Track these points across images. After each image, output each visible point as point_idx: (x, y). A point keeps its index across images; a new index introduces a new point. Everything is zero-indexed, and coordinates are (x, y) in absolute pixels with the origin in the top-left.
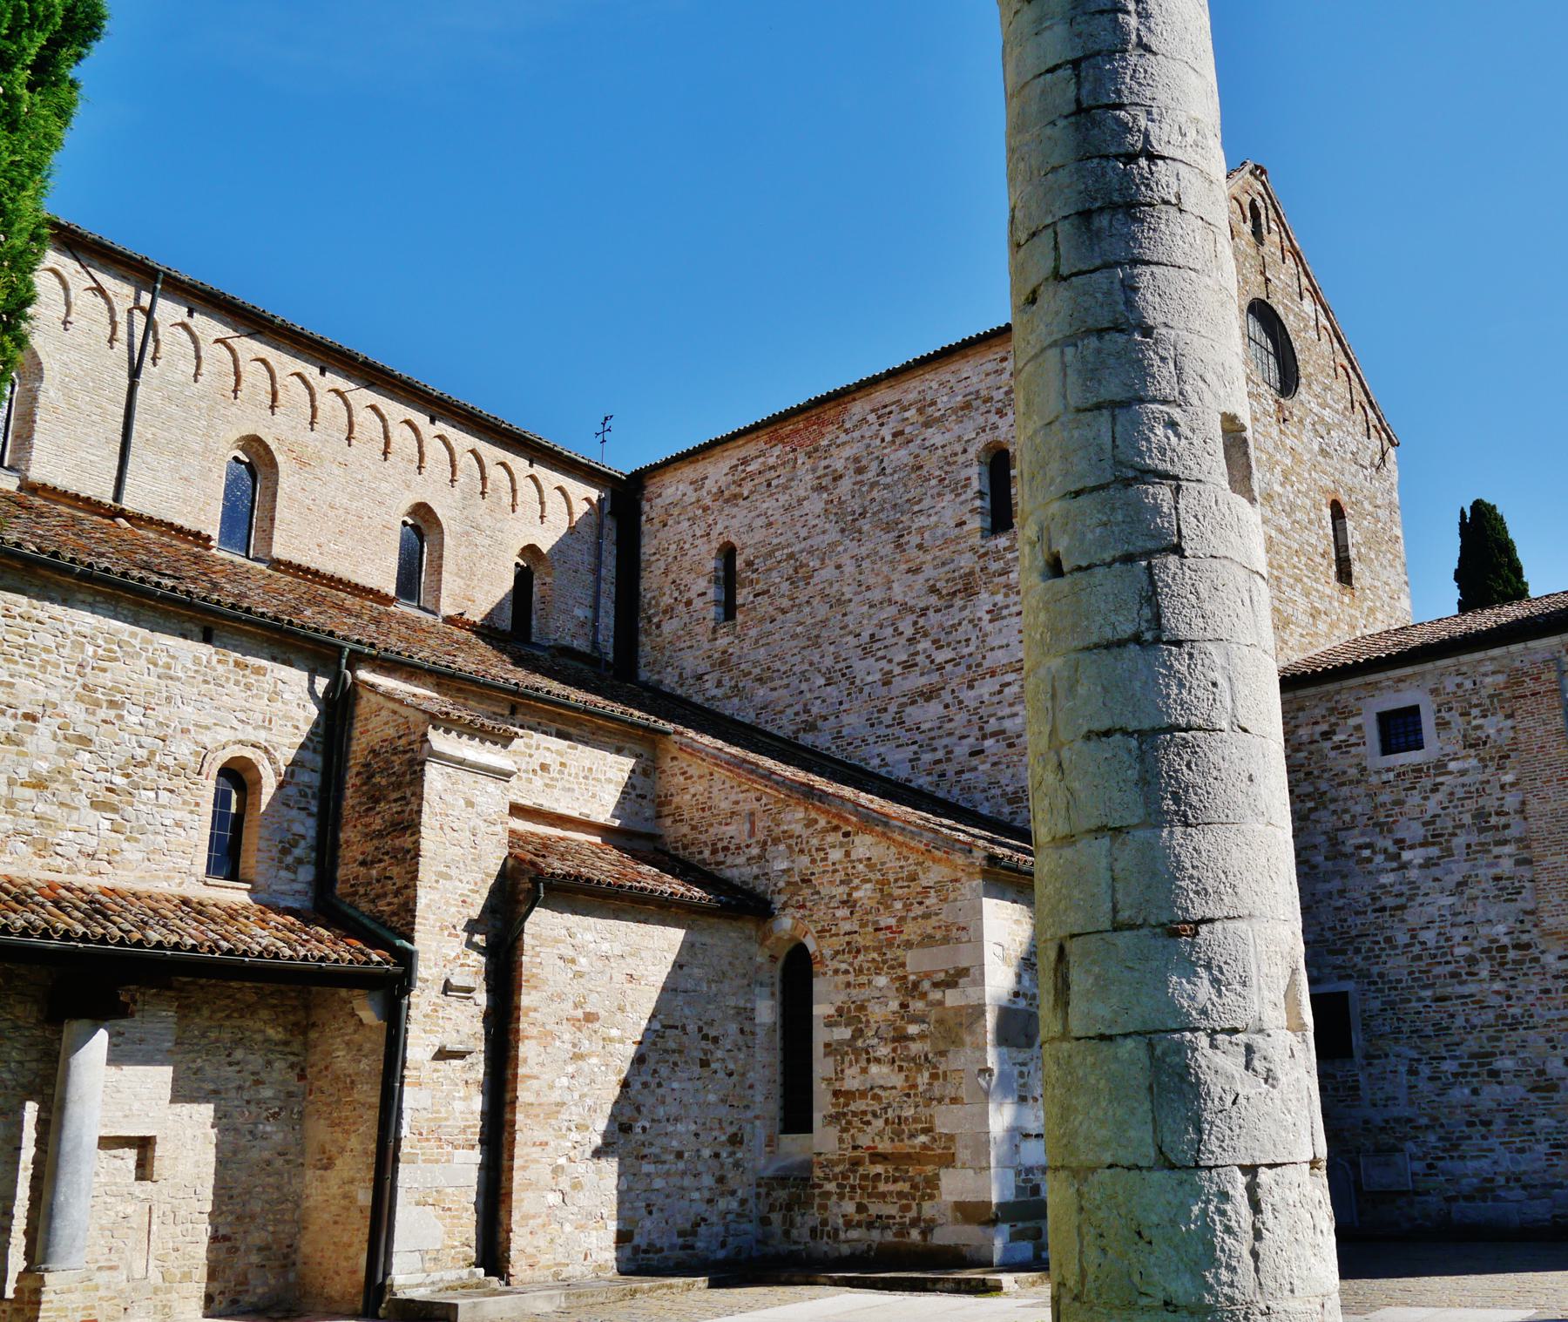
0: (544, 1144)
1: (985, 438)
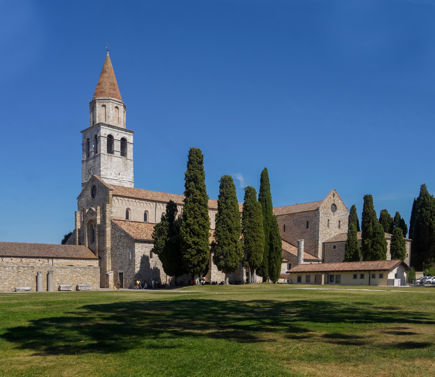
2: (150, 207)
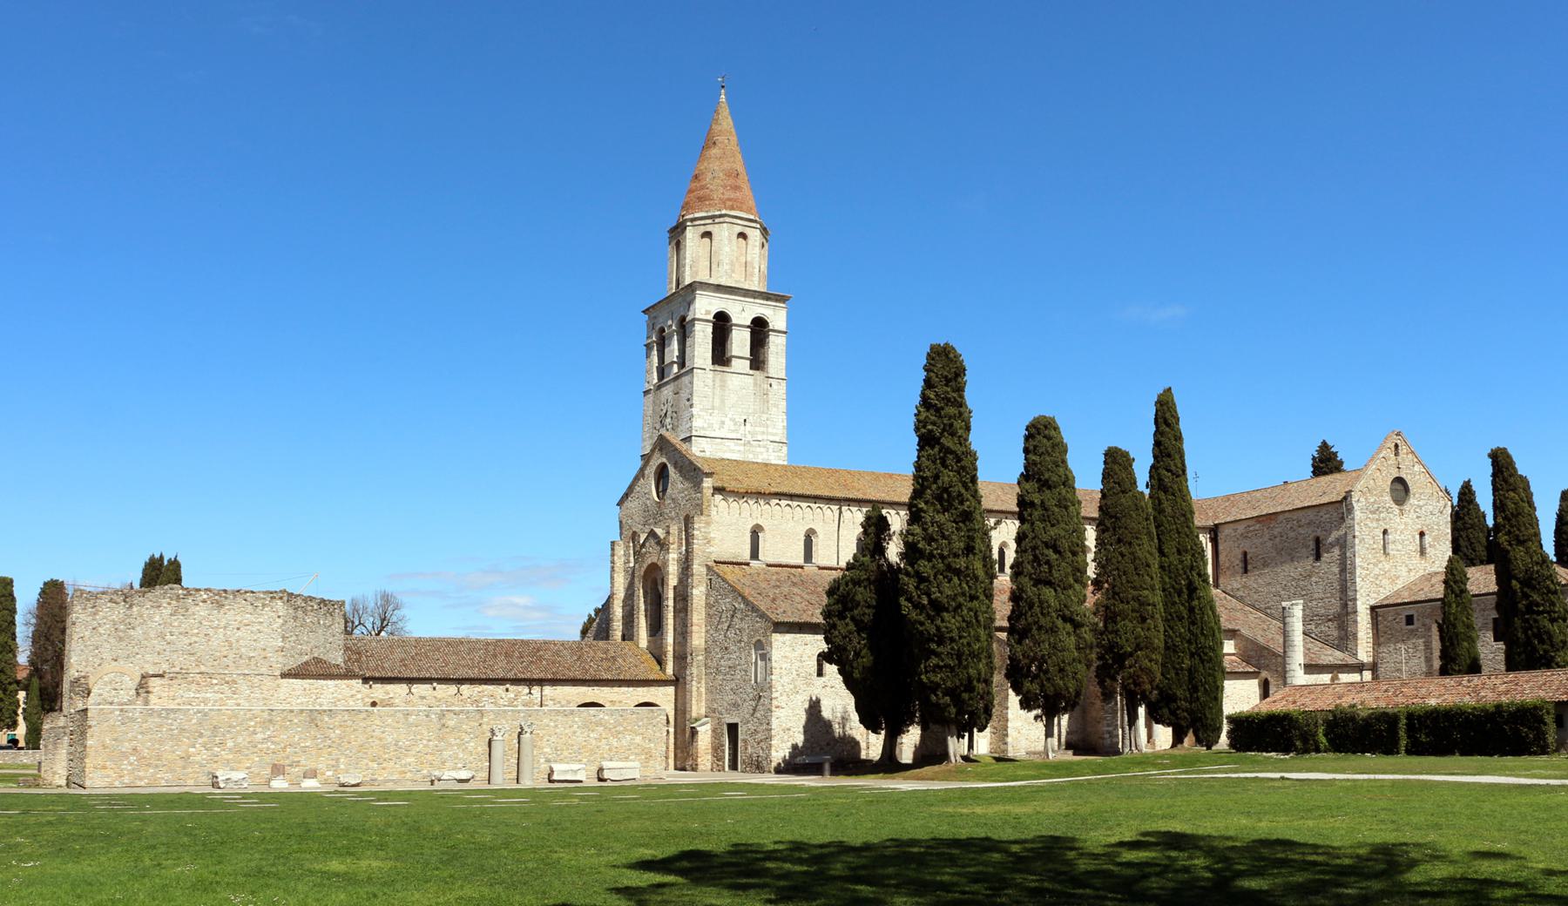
1: (1314, 534)
2: (821, 518)
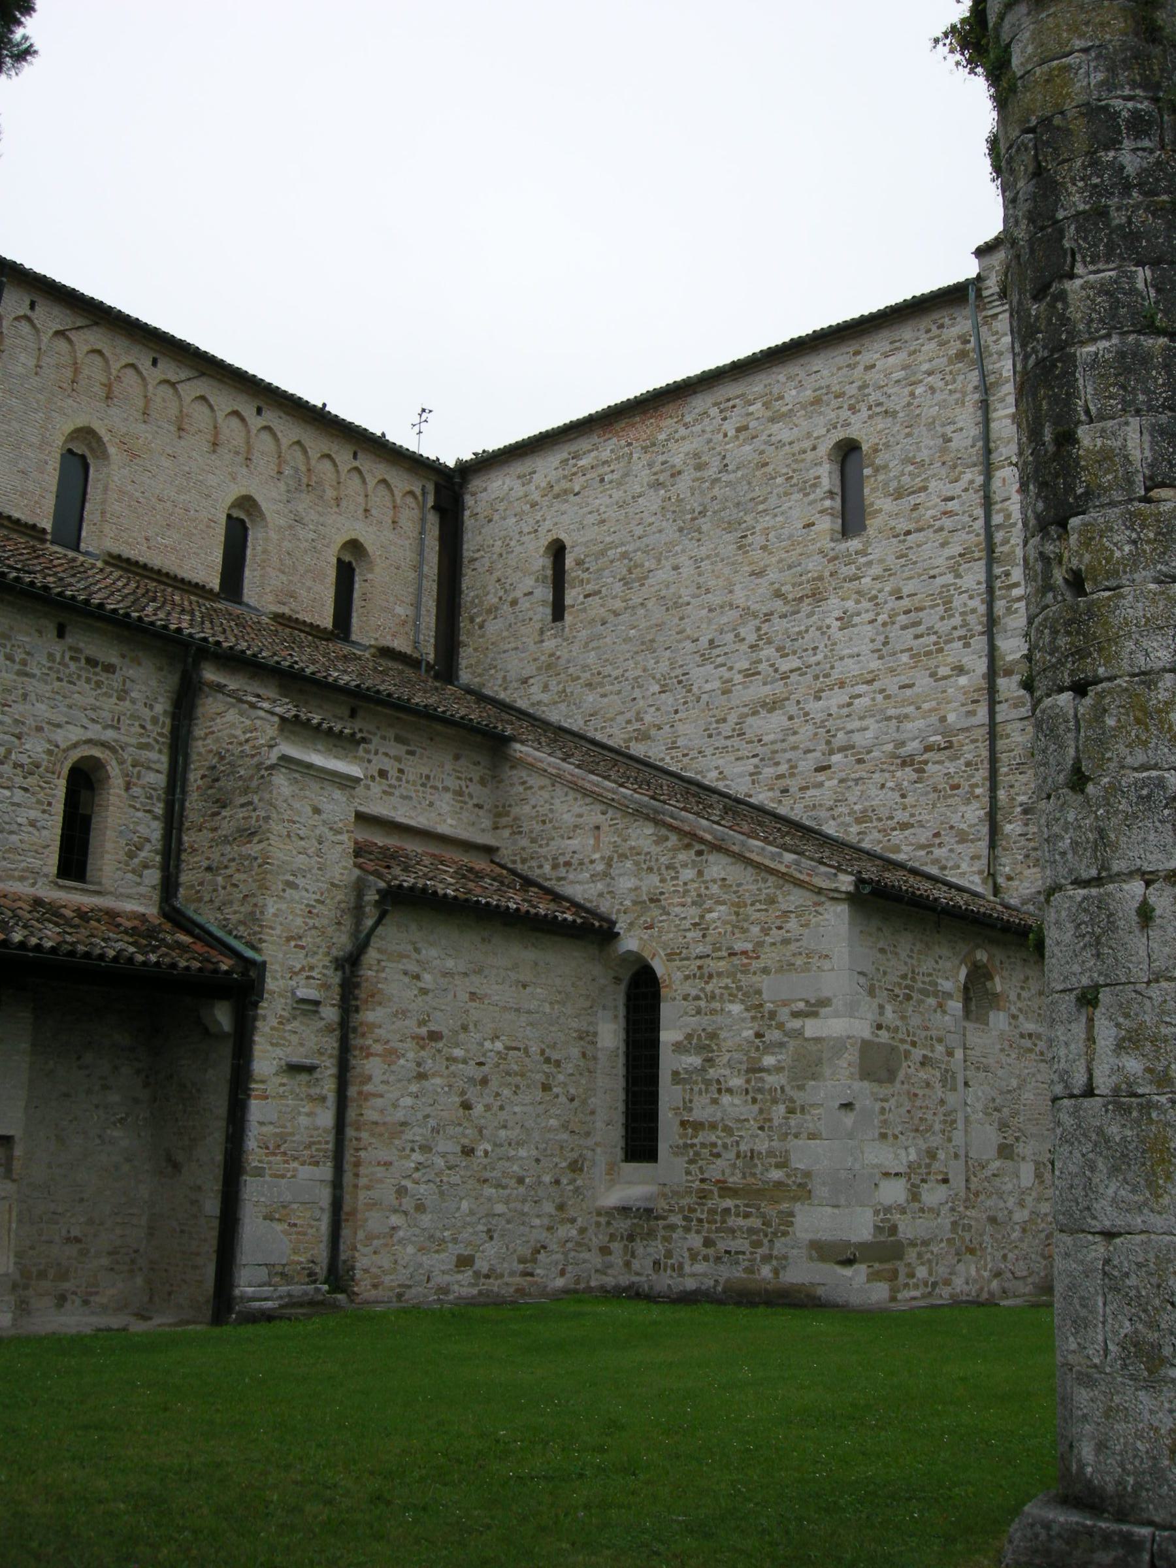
0: (388, 1164)
1: (839, 435)
